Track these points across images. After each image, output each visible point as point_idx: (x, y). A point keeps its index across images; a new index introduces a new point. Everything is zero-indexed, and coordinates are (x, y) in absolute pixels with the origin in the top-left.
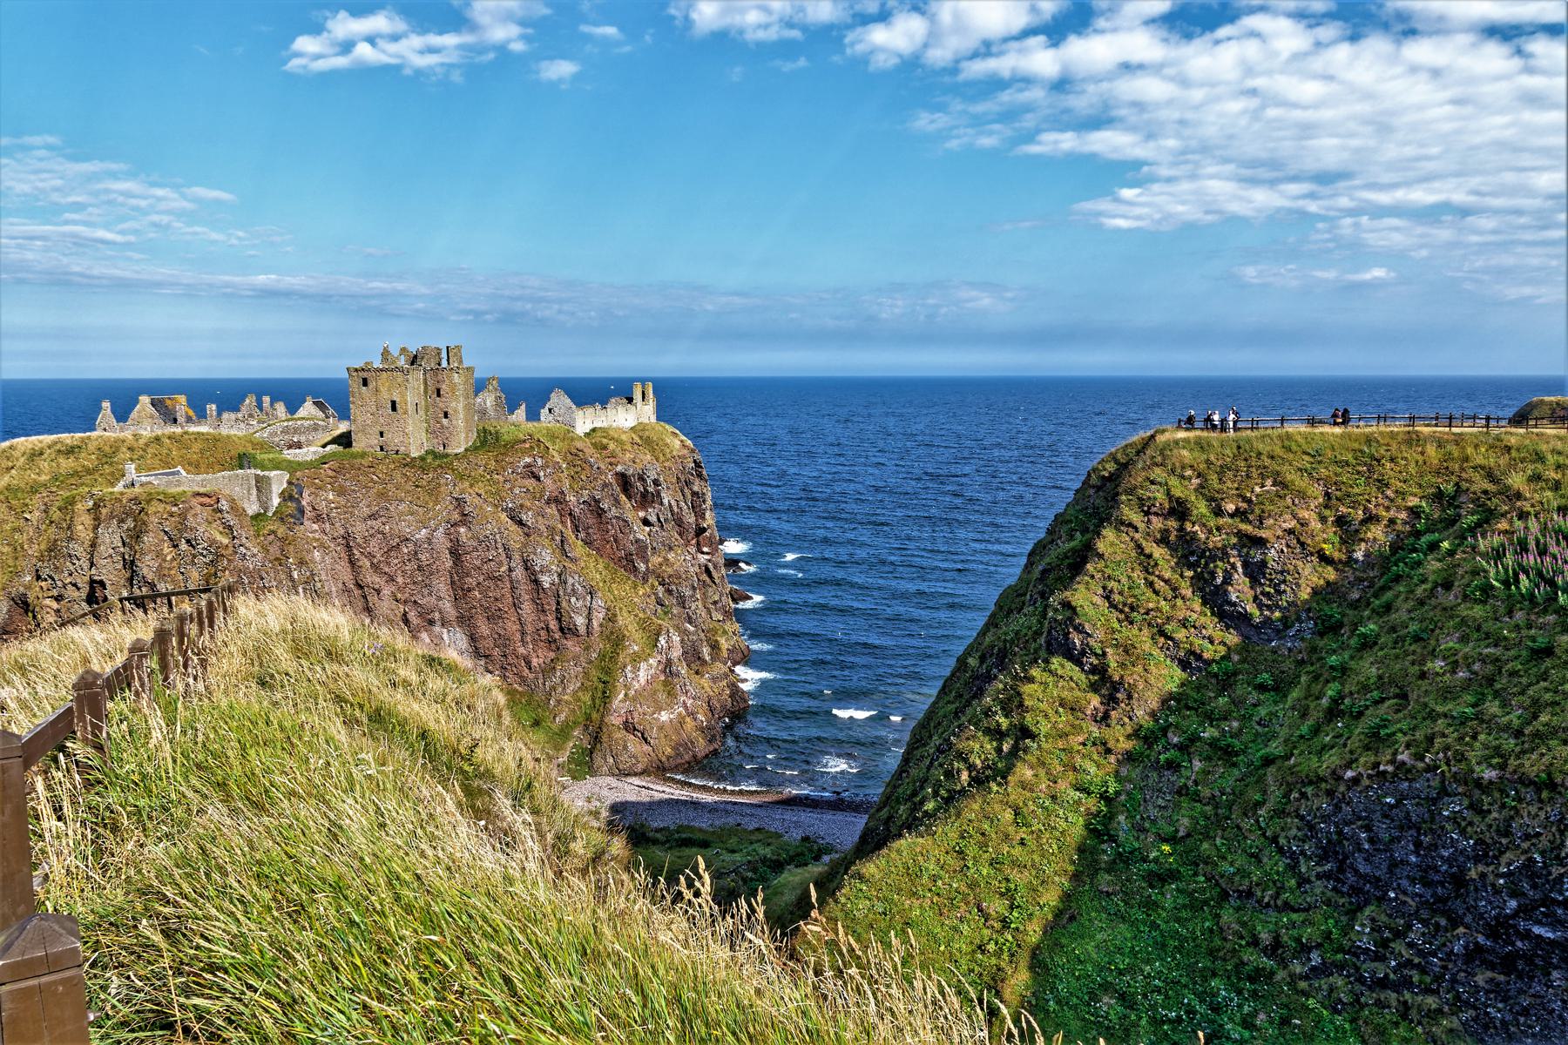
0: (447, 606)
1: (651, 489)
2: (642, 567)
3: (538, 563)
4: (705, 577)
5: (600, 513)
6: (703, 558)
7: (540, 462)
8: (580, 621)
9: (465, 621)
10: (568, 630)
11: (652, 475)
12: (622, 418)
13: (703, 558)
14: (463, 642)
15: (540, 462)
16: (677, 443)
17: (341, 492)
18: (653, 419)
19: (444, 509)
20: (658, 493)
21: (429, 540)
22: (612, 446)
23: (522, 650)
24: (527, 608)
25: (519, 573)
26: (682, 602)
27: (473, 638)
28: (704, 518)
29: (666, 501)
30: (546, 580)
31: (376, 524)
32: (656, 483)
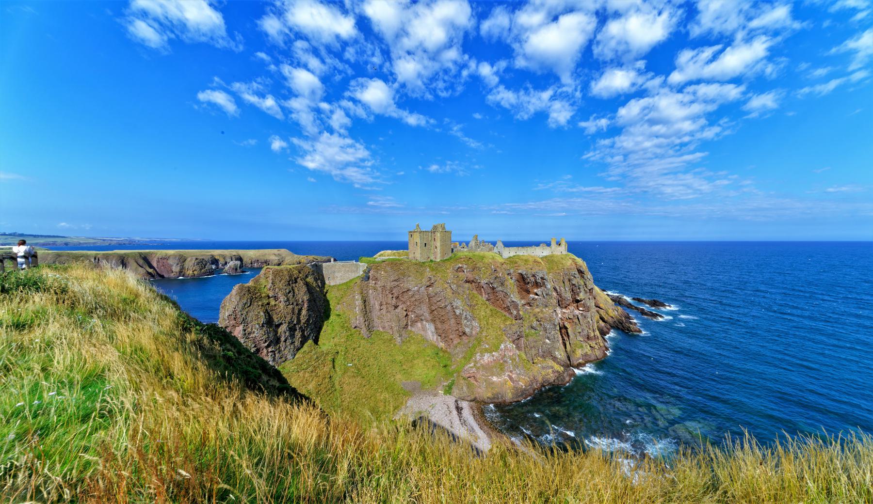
0: (427, 315)
1: (539, 281)
2: (515, 312)
3: (455, 304)
4: (576, 321)
5: (493, 288)
6: (577, 312)
7: (465, 266)
8: (467, 330)
9: (433, 321)
10: (464, 333)
11: (541, 275)
12: (541, 252)
13: (577, 312)
14: (433, 330)
15: (465, 266)
16: (571, 261)
17: (386, 272)
18: (565, 252)
19: (425, 281)
20: (544, 283)
21: (418, 291)
22: (520, 262)
23: (451, 337)
24: (453, 321)
25: (449, 307)
26: (545, 330)
27: (436, 329)
28: (578, 295)
29: (549, 286)
30: (458, 312)
31: (396, 283)
32: (542, 278)
